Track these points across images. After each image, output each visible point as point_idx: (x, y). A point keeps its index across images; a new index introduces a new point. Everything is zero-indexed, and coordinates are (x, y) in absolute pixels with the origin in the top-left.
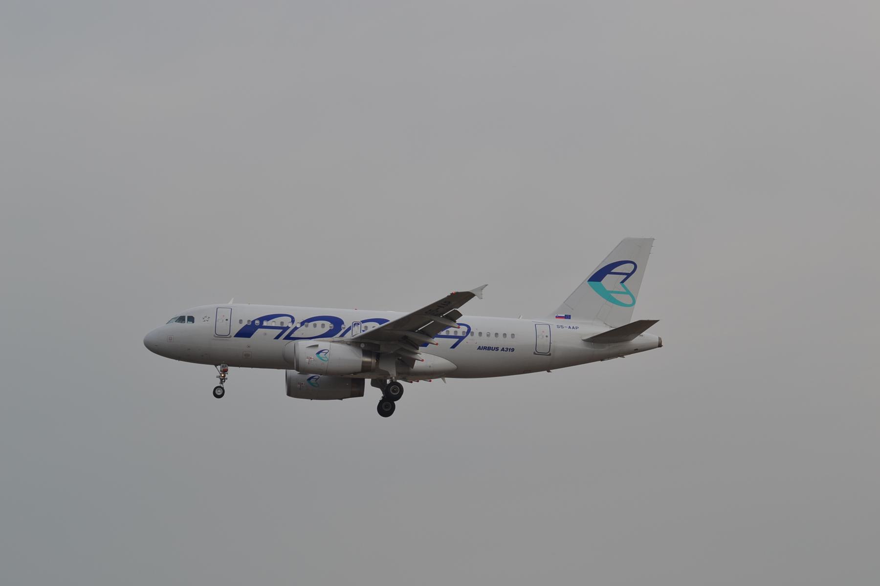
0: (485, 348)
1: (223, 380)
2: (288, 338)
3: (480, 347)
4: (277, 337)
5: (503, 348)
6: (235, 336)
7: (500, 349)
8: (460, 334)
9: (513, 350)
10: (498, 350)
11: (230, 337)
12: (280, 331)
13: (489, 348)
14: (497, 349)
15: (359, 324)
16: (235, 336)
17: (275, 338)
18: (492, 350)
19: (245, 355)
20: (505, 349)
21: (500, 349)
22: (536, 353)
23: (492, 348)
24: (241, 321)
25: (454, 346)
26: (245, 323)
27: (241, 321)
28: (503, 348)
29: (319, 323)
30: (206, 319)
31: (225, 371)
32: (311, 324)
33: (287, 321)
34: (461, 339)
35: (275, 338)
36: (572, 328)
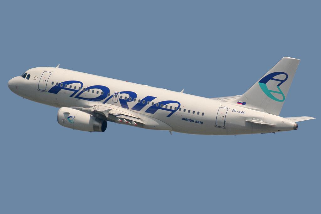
0: (186, 119)
3: (183, 118)
4: (72, 96)
6: (49, 92)
7: (195, 121)
9: (202, 123)
10: (194, 122)
13: (189, 120)
14: (193, 121)
16: (49, 92)
21: (195, 121)
24: (53, 83)
25: (169, 116)
26: (55, 84)
27: (53, 83)
29: (96, 90)
32: (91, 90)
33: (78, 85)
34: (173, 111)
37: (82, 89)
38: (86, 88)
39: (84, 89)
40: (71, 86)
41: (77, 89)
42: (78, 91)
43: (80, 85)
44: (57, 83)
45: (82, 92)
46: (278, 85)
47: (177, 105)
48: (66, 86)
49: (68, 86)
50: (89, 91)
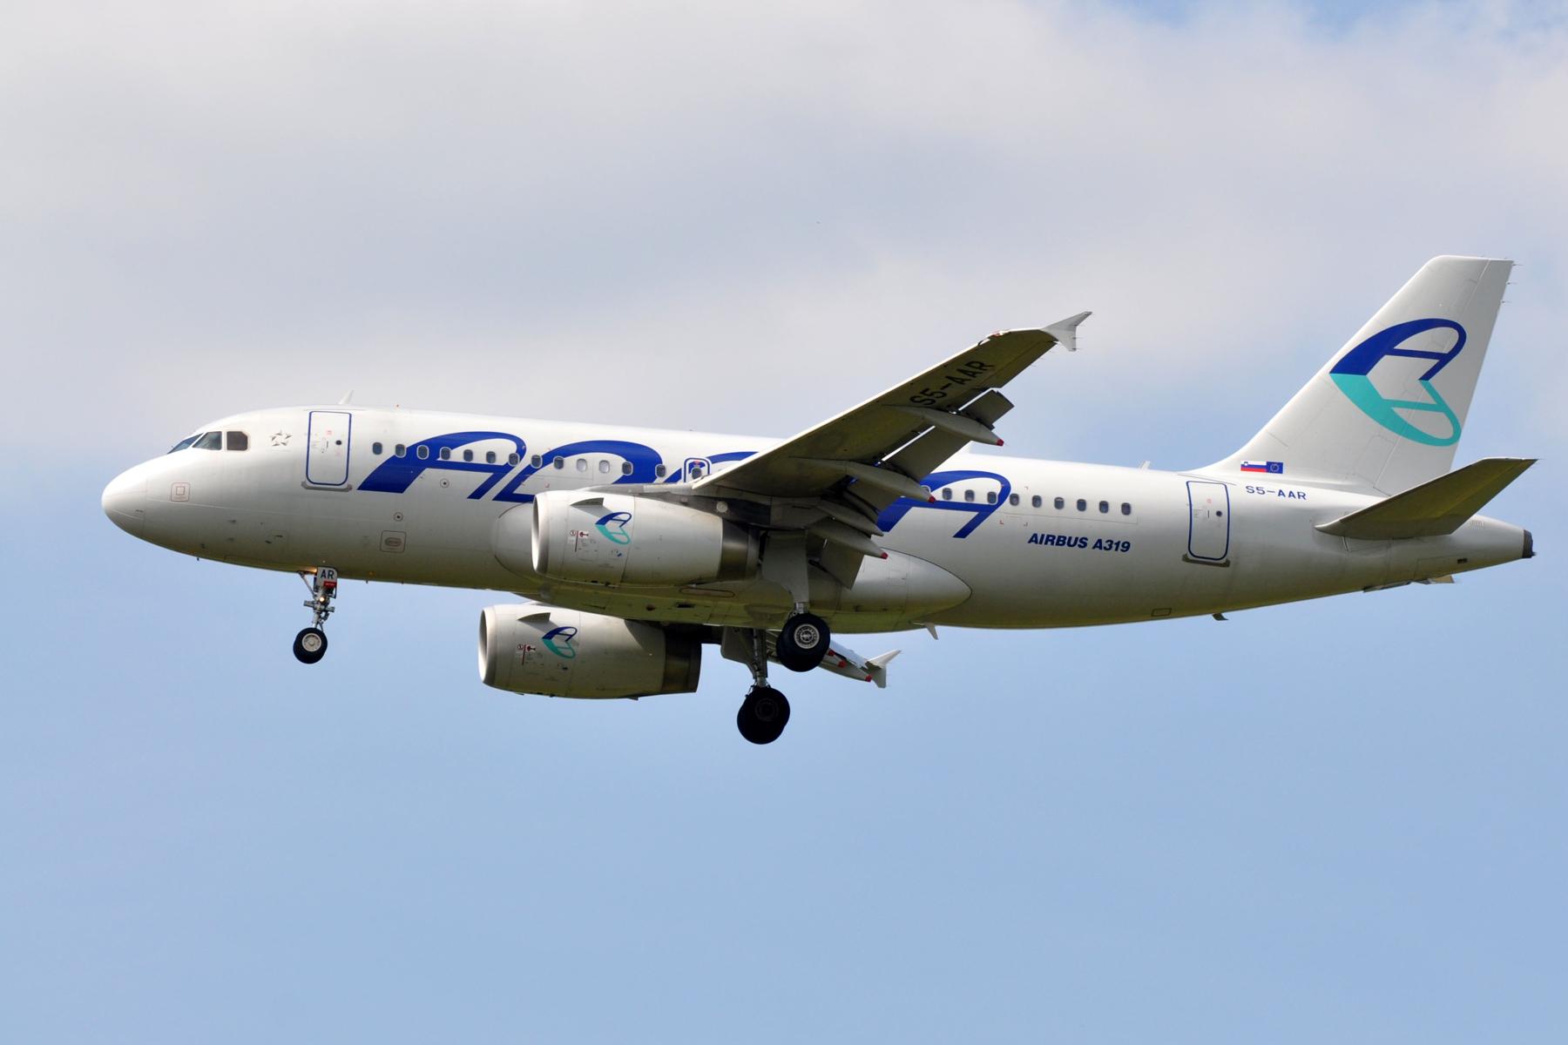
0: (1050, 539)
1: (323, 611)
2: (508, 495)
3: (1035, 535)
4: (478, 494)
5: (1100, 541)
6: (359, 489)
7: (1091, 543)
8: (981, 499)
9: (1126, 546)
10: (1085, 545)
11: (350, 488)
12: (486, 476)
13: (1061, 541)
14: (1083, 542)
15: (702, 465)
16: (359, 489)
17: (472, 497)
18: (1069, 545)
19: (388, 542)
20: (1105, 544)
21: (1091, 543)
22: (1190, 556)
23: (1070, 538)
24: (377, 448)
25: (963, 533)
26: (389, 452)
27: (377, 448)
28: (1100, 541)
29: (594, 458)
30: (279, 439)
31: (329, 589)
32: (570, 461)
33: (504, 450)
34: (984, 511)
35: (472, 497)
36: (1287, 494)
37: (526, 461)
38: (542, 452)
39: (535, 459)
40: (468, 454)
41: (501, 460)
42: (506, 469)
43: (512, 447)
44: (399, 448)
45: (529, 471)
46: (1427, 376)
47: (996, 487)
48: (447, 454)
49: (457, 455)
50: (560, 465)
